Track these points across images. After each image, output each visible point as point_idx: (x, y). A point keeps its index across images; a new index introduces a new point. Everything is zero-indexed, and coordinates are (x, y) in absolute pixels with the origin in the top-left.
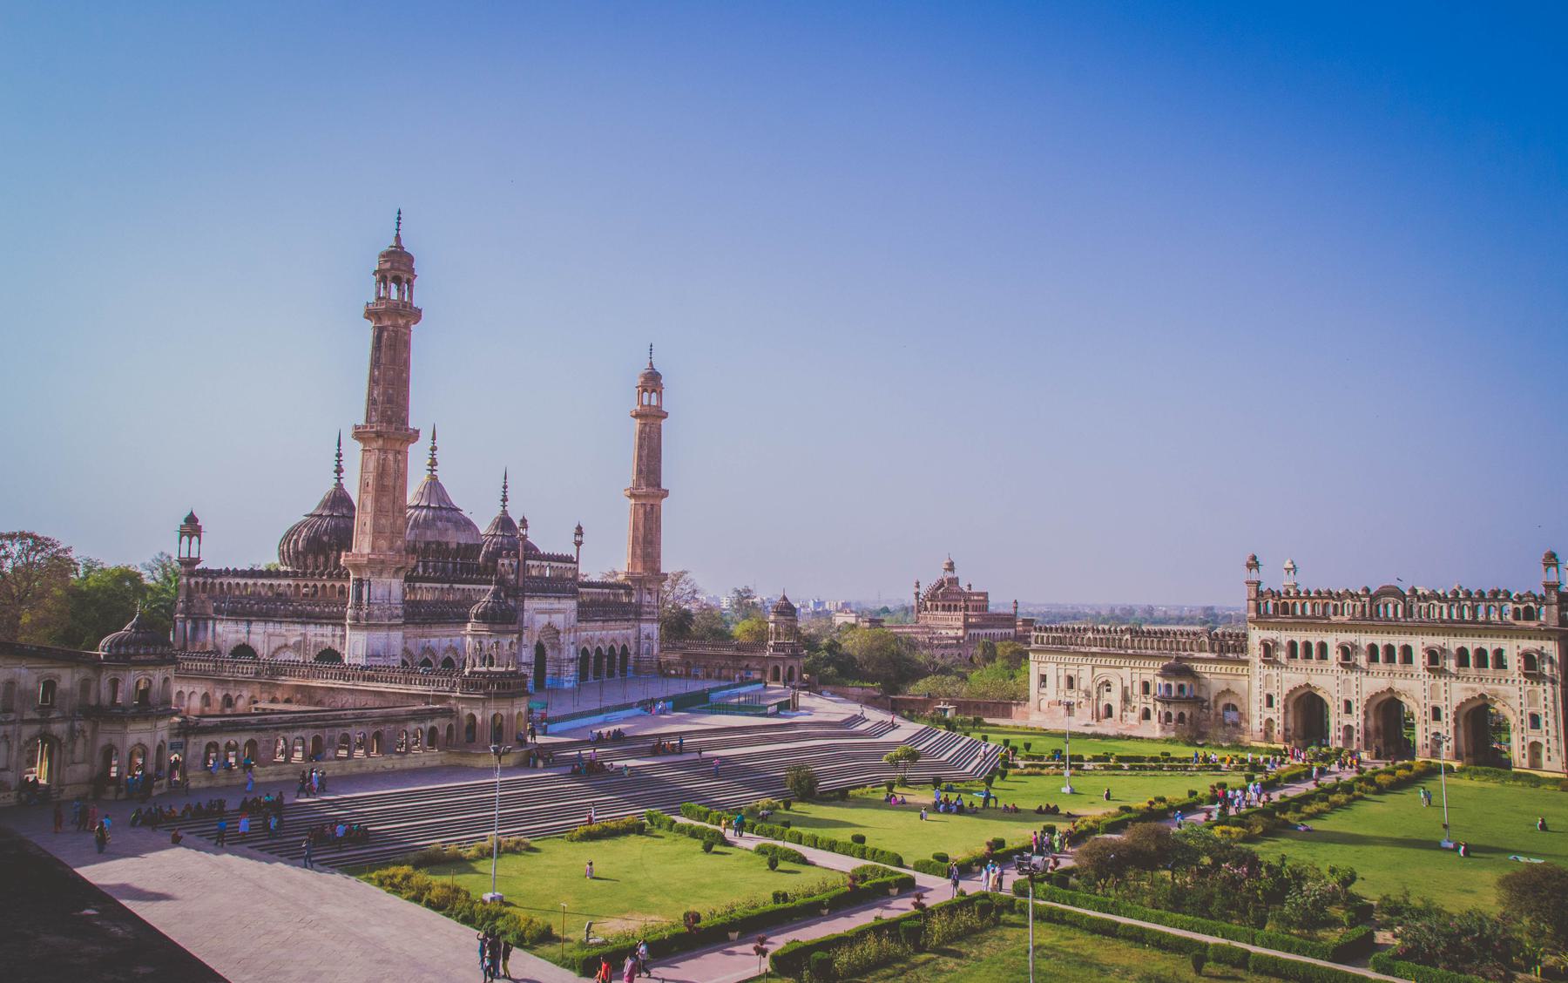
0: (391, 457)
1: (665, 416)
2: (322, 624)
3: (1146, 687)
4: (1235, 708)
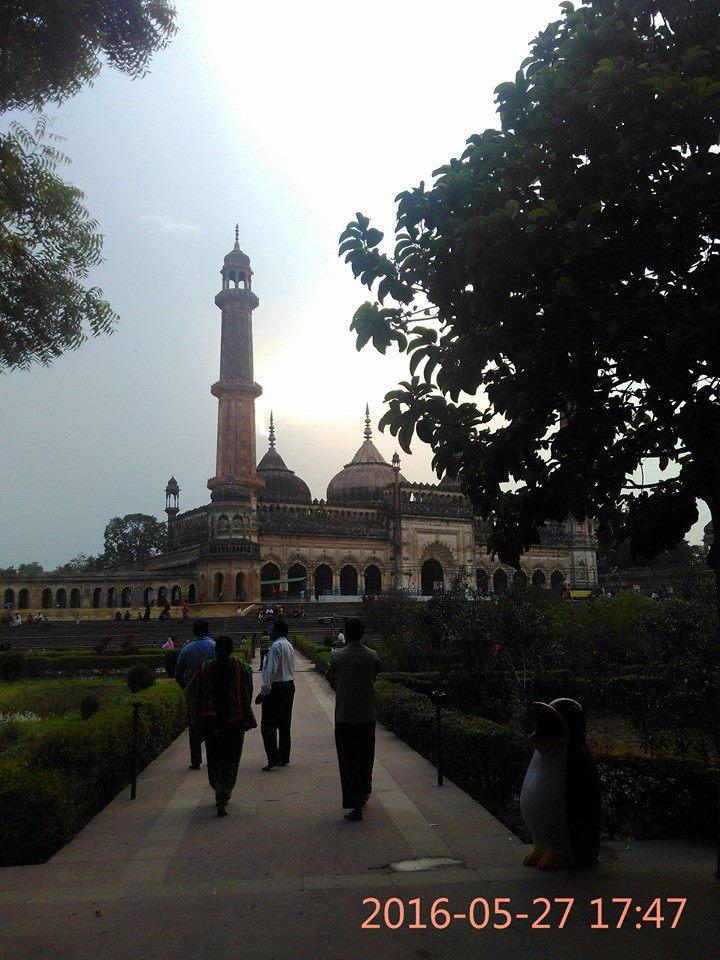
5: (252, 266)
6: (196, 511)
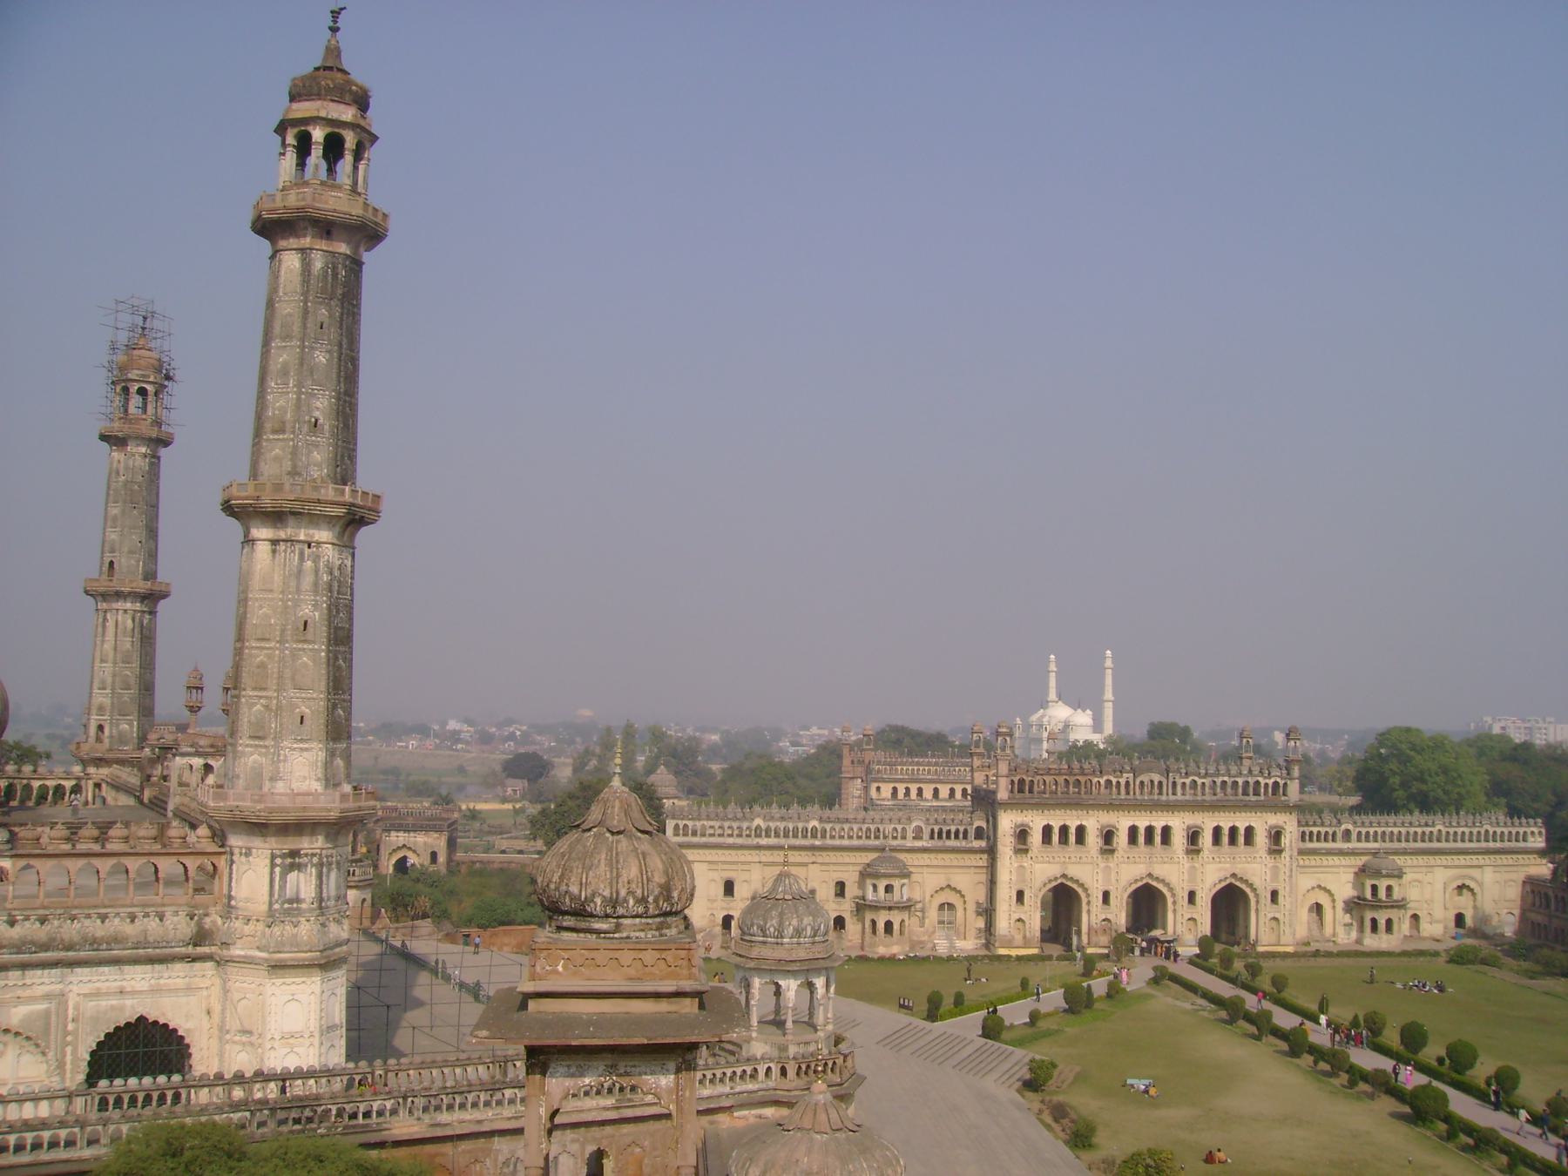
3: (840, 888)
4: (951, 906)
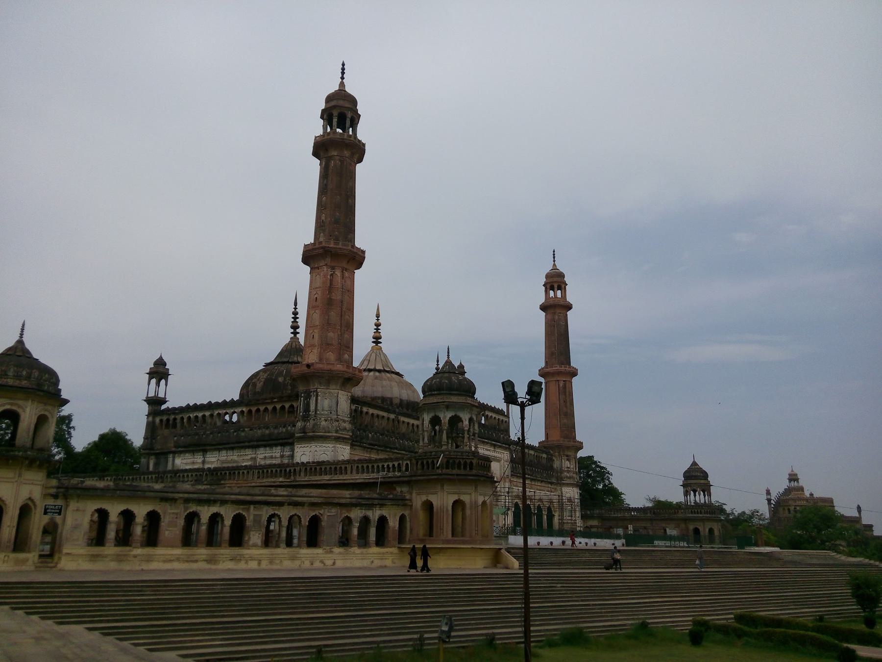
0: (338, 273)
1: (569, 307)
2: (271, 446)
5: (360, 109)
6: (196, 408)
